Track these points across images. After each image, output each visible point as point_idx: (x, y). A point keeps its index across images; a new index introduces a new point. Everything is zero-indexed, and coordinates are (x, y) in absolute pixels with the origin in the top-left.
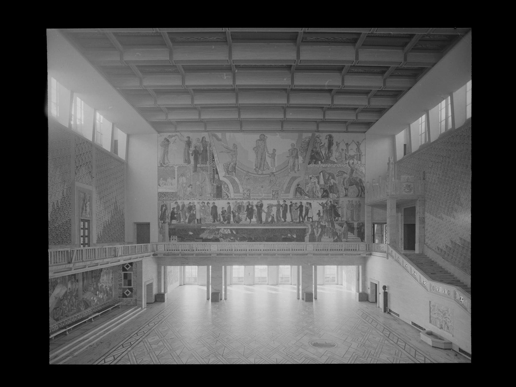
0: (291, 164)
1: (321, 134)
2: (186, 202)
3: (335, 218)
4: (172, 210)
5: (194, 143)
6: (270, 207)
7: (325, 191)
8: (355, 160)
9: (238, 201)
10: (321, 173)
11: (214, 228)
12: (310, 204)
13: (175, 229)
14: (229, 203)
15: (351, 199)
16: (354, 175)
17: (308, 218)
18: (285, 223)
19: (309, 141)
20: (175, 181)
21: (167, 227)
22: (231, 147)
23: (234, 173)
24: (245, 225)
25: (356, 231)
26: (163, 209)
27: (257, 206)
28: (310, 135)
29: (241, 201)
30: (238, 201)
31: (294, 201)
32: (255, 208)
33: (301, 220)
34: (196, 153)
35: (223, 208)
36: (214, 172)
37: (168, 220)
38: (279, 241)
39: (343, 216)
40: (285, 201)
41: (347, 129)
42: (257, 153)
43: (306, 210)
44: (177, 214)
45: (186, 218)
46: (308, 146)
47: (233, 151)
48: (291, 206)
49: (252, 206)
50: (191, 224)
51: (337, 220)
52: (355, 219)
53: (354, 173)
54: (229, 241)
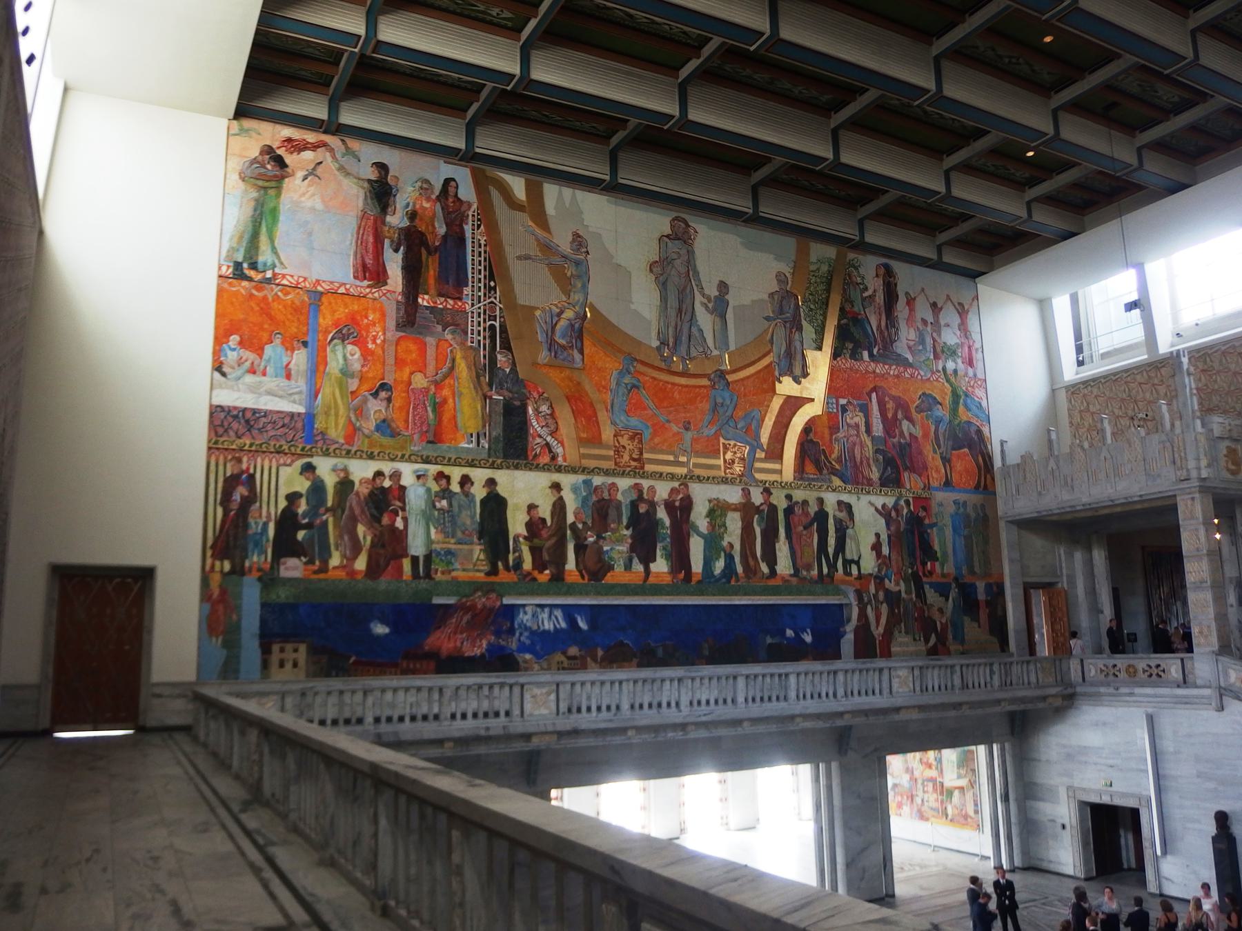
0: (780, 346)
1: (860, 257)
2: (361, 470)
3: (924, 564)
4: (283, 504)
5: (406, 196)
6: (717, 510)
7: (889, 462)
8: (959, 361)
9: (597, 480)
10: (874, 395)
11: (490, 601)
12: (849, 507)
13: (293, 607)
14: (556, 487)
15: (961, 497)
16: (963, 415)
17: (847, 563)
18: (772, 583)
19: (831, 274)
20: (300, 359)
21: (251, 596)
22: (563, 241)
23: (577, 356)
24: (627, 590)
25: (983, 614)
26: (234, 497)
27: (669, 506)
28: (830, 252)
29: (610, 480)
30: (597, 480)
31: (799, 495)
32: (662, 514)
33: (825, 570)
34: (413, 241)
35: (532, 507)
36: (493, 338)
37: (258, 559)
38: (756, 660)
39: (945, 554)
40: (767, 492)
41: (939, 249)
42: (663, 286)
43: (837, 531)
44: (309, 526)
45: (356, 548)
46: (828, 290)
47: (570, 268)
48: (789, 511)
49: (653, 505)
50: (384, 583)
51: (931, 573)
52: (977, 569)
53: (961, 407)
54: (561, 668)
